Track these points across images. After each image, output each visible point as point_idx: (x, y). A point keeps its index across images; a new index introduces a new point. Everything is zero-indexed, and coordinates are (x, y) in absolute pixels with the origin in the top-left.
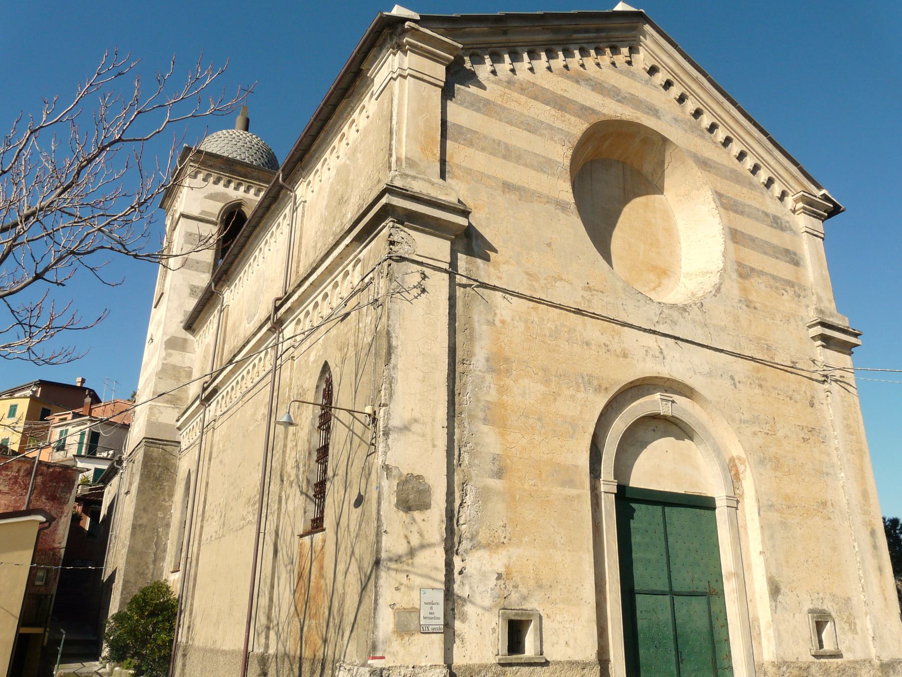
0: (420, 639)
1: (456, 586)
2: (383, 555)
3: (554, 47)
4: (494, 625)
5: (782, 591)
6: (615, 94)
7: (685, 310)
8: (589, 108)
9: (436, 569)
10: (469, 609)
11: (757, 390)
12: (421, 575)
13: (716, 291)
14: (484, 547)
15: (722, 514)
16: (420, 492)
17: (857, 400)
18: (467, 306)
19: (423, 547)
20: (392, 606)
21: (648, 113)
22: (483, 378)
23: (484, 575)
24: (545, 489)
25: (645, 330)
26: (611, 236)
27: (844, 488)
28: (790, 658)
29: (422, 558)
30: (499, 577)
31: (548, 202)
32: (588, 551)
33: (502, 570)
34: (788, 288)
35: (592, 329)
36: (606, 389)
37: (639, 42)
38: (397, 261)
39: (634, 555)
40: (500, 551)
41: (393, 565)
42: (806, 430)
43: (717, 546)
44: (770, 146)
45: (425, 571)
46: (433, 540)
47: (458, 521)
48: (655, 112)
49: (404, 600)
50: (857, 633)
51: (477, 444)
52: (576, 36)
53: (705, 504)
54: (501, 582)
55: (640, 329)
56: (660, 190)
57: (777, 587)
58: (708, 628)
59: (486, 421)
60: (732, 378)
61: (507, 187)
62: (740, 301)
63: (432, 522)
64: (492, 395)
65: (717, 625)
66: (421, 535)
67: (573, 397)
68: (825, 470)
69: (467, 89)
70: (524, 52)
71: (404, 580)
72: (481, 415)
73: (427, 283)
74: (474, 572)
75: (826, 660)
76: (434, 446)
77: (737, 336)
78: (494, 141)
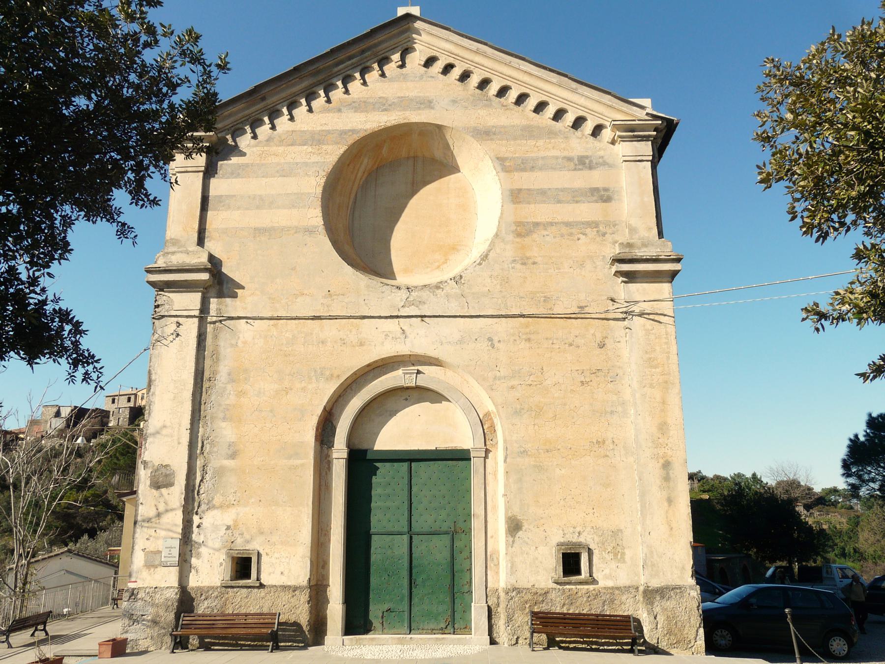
0: (161, 571)
1: (194, 536)
2: (139, 518)
3: (314, 89)
4: (221, 560)
5: (524, 528)
6: (384, 105)
7: (438, 287)
8: (349, 131)
9: (176, 525)
10: (203, 550)
11: (523, 345)
12: (165, 530)
13: (483, 259)
14: (218, 508)
15: (476, 463)
16: (166, 476)
17: (671, 330)
18: (216, 337)
19: (167, 511)
20: (144, 550)
21: (419, 108)
22: (225, 388)
23: (216, 528)
24: (272, 462)
25: (386, 317)
26: (392, 232)
27: (634, 426)
28: (524, 583)
29: (167, 519)
30: (228, 528)
31: (296, 232)
32: (308, 505)
33: (230, 523)
34: (588, 231)
35: (330, 329)
36: (338, 376)
37: (412, 41)
38: (159, 319)
39: (373, 505)
40: (230, 509)
41: (146, 524)
42: (587, 374)
43: (468, 491)
44: (574, 85)
45: (169, 527)
46: (174, 507)
47: (198, 492)
48: (428, 104)
49: (151, 546)
50: (624, 562)
51: (216, 437)
52: (336, 69)
53: (462, 456)
54: (229, 532)
55: (380, 317)
56: (454, 169)
57: (517, 525)
58: (449, 559)
59: (224, 419)
60: (490, 339)
61: (259, 231)
62: (514, 261)
63: (176, 495)
64: (231, 399)
65: (459, 558)
66: (166, 503)
67: (304, 389)
68: (609, 410)
69: (229, 162)
70: (283, 107)
71: (153, 533)
72: (221, 415)
73: (181, 330)
74: (208, 525)
75: (573, 587)
76: (179, 443)
77: (504, 297)
78: (249, 197)
